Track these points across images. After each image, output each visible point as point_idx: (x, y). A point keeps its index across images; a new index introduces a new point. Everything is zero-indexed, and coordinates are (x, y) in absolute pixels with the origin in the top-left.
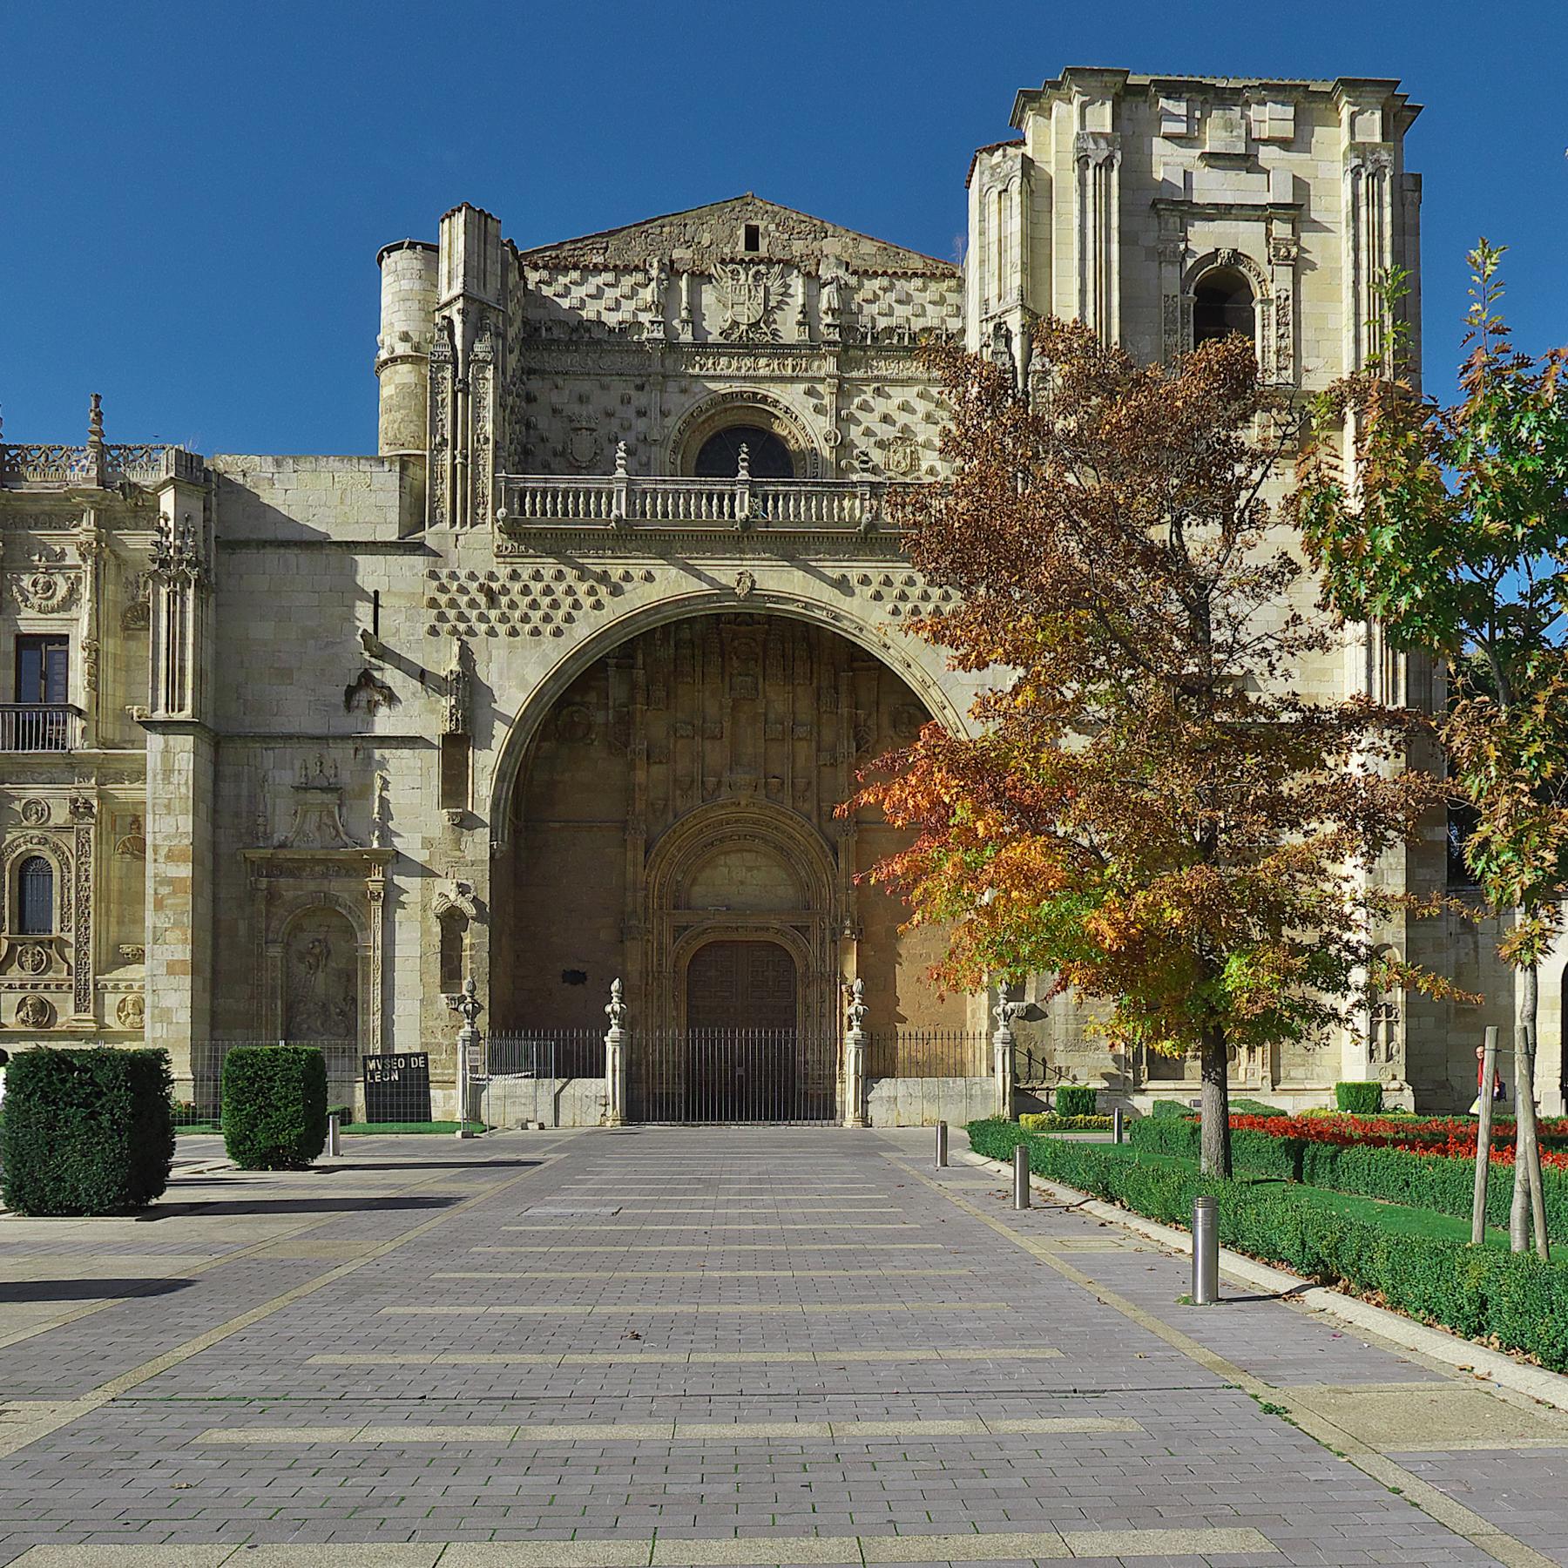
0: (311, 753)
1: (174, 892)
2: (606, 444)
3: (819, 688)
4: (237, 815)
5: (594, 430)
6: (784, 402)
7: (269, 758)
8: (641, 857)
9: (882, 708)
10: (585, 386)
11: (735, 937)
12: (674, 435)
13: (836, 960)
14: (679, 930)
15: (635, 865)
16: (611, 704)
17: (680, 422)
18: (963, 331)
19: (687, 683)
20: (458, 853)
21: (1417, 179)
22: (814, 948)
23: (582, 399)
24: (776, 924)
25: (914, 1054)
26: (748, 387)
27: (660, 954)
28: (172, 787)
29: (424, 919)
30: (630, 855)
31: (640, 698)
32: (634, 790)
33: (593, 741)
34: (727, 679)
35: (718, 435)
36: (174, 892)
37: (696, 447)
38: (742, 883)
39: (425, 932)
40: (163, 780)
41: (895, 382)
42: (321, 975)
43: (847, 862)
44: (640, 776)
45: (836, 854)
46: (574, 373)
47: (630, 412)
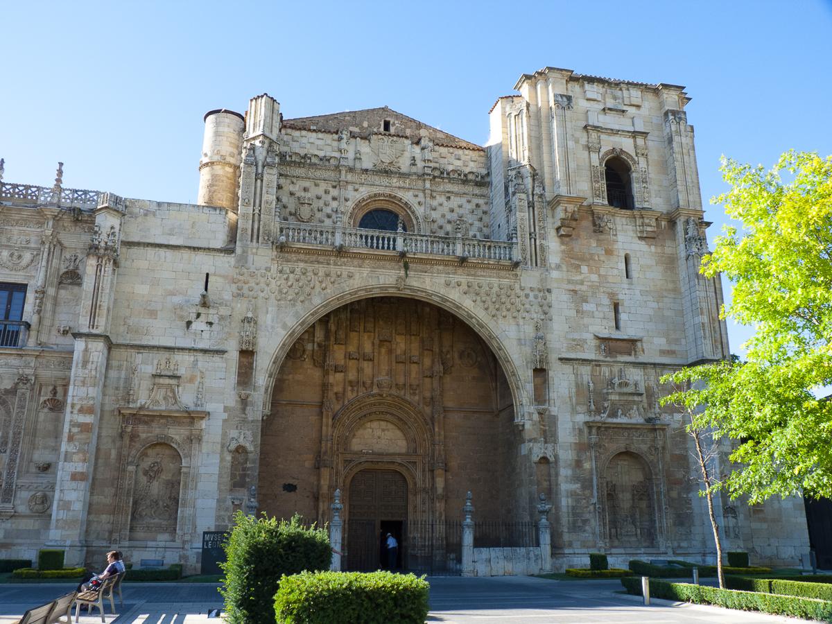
0: (163, 356)
1: (81, 431)
2: (316, 212)
4: (117, 388)
5: (311, 205)
6: (405, 199)
7: (139, 358)
9: (454, 349)
10: (307, 184)
11: (376, 467)
14: (347, 462)
15: (327, 426)
16: (316, 339)
17: (354, 205)
18: (488, 174)
19: (356, 331)
20: (244, 416)
21: (692, 127)
22: (419, 474)
24: (399, 461)
26: (388, 191)
28: (87, 371)
29: (222, 453)
30: (324, 420)
31: (332, 339)
32: (328, 386)
33: (305, 359)
34: (377, 330)
35: (370, 212)
36: (81, 431)
37: (360, 216)
38: (379, 438)
39: (222, 460)
40: (82, 367)
41: (457, 194)
42: (155, 484)
43: (439, 428)
44: (331, 379)
45: (433, 424)
46: (302, 178)
47: (329, 198)
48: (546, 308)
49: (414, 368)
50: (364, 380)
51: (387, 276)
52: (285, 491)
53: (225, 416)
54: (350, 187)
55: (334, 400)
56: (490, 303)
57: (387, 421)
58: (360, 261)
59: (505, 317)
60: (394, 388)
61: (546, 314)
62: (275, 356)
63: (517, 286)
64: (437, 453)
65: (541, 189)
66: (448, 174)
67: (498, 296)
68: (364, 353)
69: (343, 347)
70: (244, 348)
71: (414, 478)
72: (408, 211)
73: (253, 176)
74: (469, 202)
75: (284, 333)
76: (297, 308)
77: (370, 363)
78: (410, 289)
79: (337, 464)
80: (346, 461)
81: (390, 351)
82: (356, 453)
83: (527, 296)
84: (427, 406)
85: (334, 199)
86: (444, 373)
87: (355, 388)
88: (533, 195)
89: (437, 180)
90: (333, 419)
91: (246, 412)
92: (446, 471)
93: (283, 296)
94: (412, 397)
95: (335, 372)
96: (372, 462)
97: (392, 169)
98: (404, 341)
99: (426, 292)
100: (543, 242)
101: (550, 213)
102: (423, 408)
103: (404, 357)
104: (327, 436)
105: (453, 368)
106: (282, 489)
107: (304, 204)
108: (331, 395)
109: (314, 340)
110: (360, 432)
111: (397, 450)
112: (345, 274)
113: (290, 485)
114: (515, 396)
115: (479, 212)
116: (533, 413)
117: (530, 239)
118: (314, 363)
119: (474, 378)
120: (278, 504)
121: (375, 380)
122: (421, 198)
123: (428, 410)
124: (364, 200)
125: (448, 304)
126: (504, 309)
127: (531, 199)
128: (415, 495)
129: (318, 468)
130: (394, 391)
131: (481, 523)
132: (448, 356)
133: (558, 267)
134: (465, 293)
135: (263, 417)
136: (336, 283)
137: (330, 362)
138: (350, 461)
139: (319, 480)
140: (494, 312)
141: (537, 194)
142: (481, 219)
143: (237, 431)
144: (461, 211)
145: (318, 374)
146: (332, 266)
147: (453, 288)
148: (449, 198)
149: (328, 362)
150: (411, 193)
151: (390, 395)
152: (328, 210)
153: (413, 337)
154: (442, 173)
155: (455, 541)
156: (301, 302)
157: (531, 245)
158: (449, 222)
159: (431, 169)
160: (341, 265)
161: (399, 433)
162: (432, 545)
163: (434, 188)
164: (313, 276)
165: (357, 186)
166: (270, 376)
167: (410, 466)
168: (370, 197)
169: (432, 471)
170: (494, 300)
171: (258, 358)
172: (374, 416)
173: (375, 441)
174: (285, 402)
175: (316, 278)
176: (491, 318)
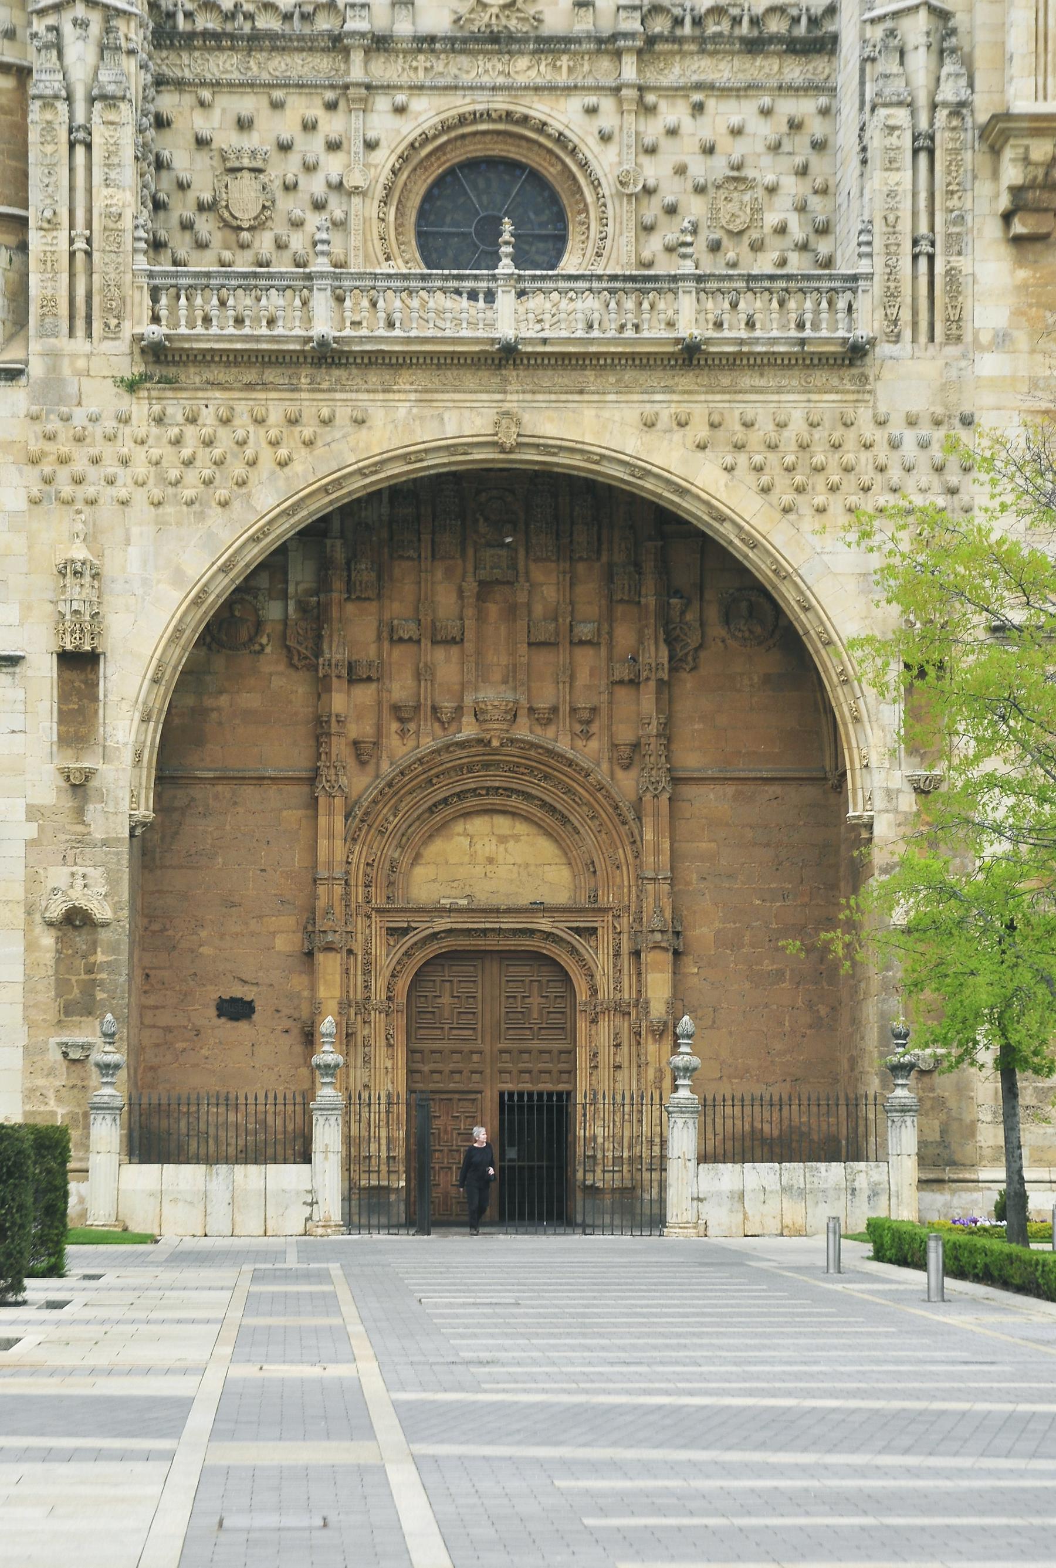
2: (279, 194)
3: (610, 565)
5: (259, 171)
6: (556, 125)
10: (248, 104)
11: (481, 943)
12: (385, 174)
13: (639, 981)
15: (331, 836)
16: (291, 589)
17: (394, 157)
19: (409, 558)
23: (244, 125)
24: (544, 924)
25: (758, 1125)
26: (500, 103)
27: (366, 972)
30: (322, 821)
31: (338, 584)
32: (328, 722)
34: (470, 552)
35: (451, 172)
38: (491, 861)
41: (725, 92)
43: (656, 832)
44: (339, 702)
48: (953, 478)
49: (586, 660)
51: (467, 413)
52: (223, 1020)
53: (31, 830)
54: (382, 103)
55: (351, 763)
56: (778, 471)
57: (514, 814)
58: (387, 375)
59: (821, 510)
60: (523, 720)
61: (953, 491)
62: (154, 662)
63: (864, 416)
64: (649, 905)
65: (963, 82)
66: (697, 22)
67: (803, 447)
68: (433, 622)
69: (373, 607)
70: (69, 647)
72: (568, 161)
73: (63, 136)
74: (766, 112)
75: (177, 595)
76: (209, 522)
77: (455, 650)
78: (537, 446)
79: (367, 941)
80: (391, 931)
81: (511, 612)
83: (895, 445)
84: (626, 768)
85: (333, 146)
86: (670, 670)
87: (412, 726)
88: (934, 107)
89: (659, 47)
90: (347, 818)
91: (87, 819)
92: (677, 953)
93: (170, 490)
94: (579, 743)
95: (351, 681)
96: (469, 931)
97: (513, 24)
99: (582, 452)
100: (956, 261)
101: (984, 160)
103: (552, 627)
105: (702, 654)
106: (213, 1012)
107: (240, 170)
108: (339, 748)
109: (285, 591)
110: (437, 847)
112: (343, 414)
113: (234, 1001)
114: (849, 742)
115: (801, 144)
116: (899, 791)
117: (915, 257)
118: (290, 658)
119: (767, 679)
120: (204, 1052)
121: (468, 700)
122: (608, 119)
123: (627, 783)
124: (426, 139)
125: (649, 484)
126: (821, 487)
127: (923, 125)
128: (594, 1021)
129: (310, 954)
130: (523, 731)
131: (785, 1098)
133: (1002, 340)
134: (702, 447)
135: (132, 829)
136: (319, 443)
137: (336, 653)
140: (788, 498)
141: (945, 104)
142: (803, 171)
143: (66, 870)
144: (738, 149)
145: (300, 691)
146: (304, 395)
147: (665, 432)
148: (699, 108)
149: (328, 656)
150: (574, 105)
151: (512, 741)
152: (316, 186)
153: (581, 568)
154: (678, 22)
156: (220, 503)
157: (915, 278)
158: (700, 190)
159: (637, 15)
160: (329, 390)
161: (546, 847)
163: (652, 77)
164: (251, 429)
165: (401, 98)
166: (145, 719)
167: (575, 940)
168: (446, 127)
169: (637, 954)
170: (790, 459)
171: (109, 673)
172: (471, 802)
173: (479, 870)
174: (211, 775)
175: (262, 431)
176: (778, 515)
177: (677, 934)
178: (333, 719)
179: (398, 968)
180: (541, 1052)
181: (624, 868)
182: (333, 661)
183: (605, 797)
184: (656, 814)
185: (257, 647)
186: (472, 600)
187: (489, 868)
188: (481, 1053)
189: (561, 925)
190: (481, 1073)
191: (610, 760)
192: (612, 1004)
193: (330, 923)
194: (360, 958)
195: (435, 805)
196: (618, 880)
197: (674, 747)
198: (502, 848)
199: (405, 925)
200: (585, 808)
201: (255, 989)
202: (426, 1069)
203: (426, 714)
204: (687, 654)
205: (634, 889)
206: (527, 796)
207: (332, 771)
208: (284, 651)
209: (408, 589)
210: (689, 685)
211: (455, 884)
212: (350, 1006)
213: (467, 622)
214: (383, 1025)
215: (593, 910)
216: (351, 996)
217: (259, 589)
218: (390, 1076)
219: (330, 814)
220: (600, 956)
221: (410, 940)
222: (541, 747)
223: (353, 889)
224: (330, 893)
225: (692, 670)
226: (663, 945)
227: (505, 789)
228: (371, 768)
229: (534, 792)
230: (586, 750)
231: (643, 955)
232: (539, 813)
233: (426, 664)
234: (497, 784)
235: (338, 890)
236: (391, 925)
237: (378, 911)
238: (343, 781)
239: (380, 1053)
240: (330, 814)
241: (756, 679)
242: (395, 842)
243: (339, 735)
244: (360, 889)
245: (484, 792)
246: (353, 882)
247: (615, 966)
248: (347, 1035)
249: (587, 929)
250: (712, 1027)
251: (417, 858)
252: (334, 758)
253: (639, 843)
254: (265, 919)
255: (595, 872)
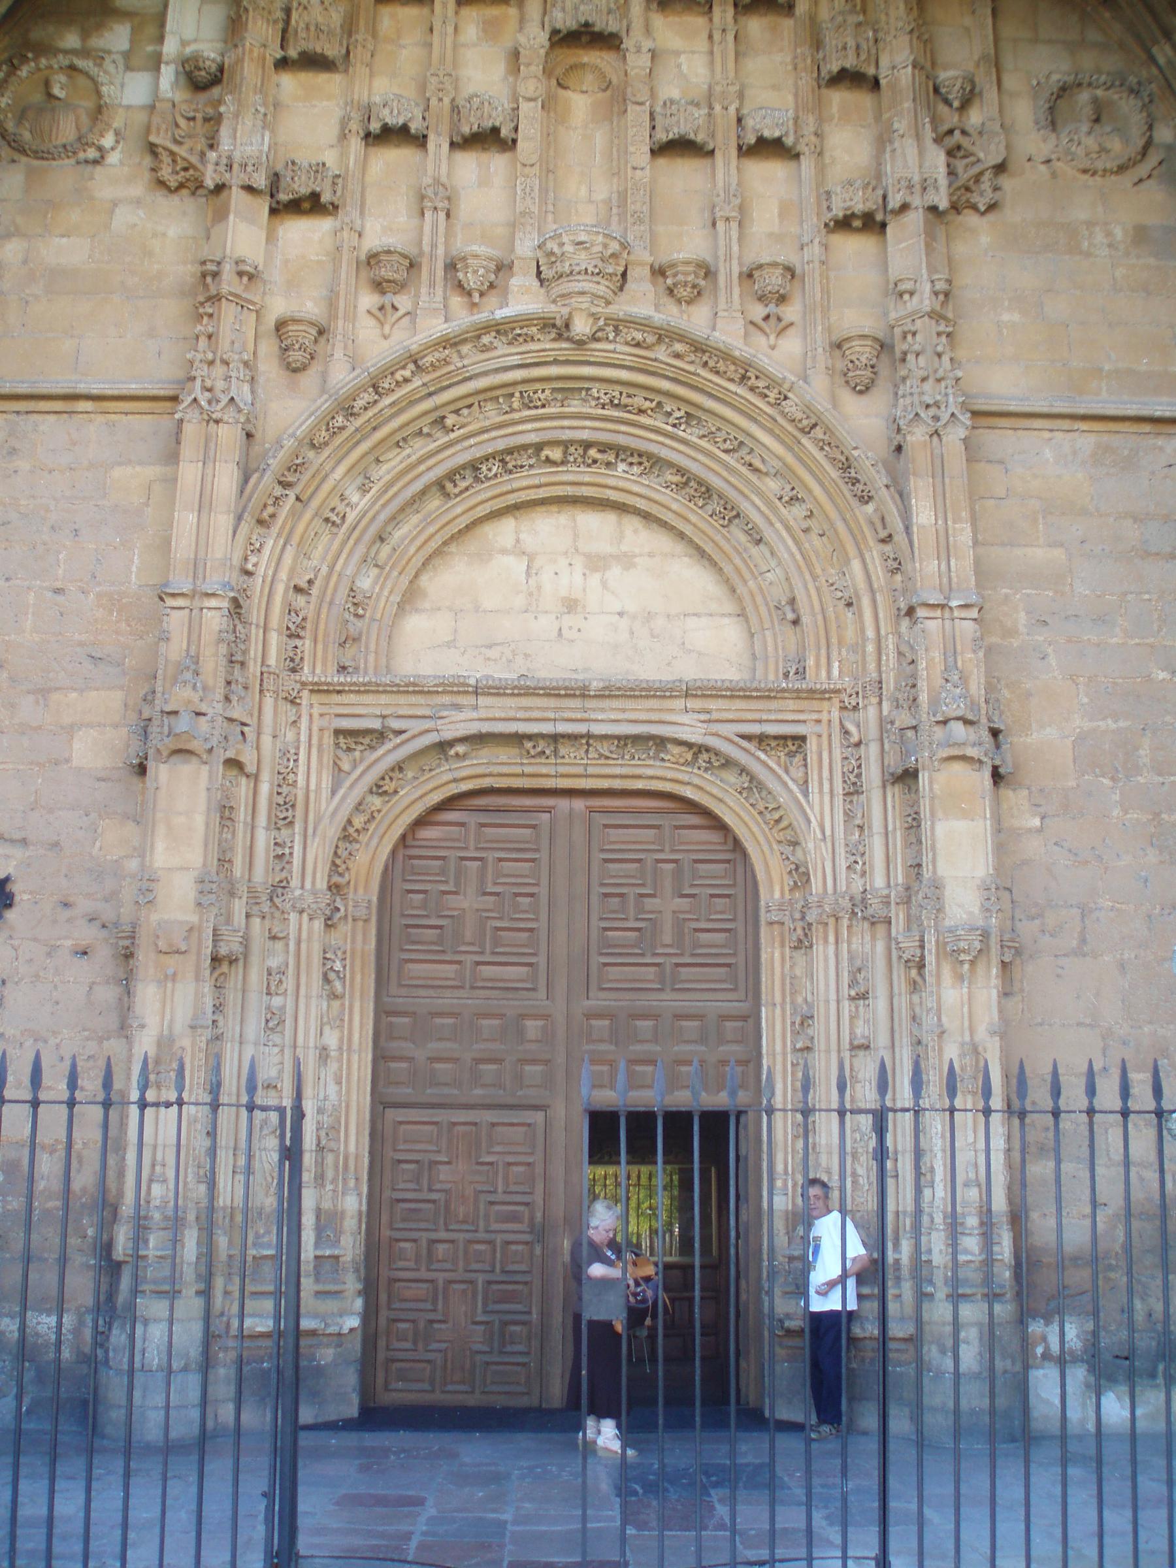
8: (226, 479)
9: (1010, 82)
15: (204, 504)
16: (170, 47)
30: (189, 472)
38: (571, 605)
50: (461, 245)
55: (269, 368)
64: (930, 665)
68: (455, 109)
71: (795, 844)
77: (497, 162)
79: (288, 755)
82: (414, 688)
87: (403, 302)
92: (997, 776)
94: (761, 340)
96: (517, 739)
98: (702, 44)
102: (835, 402)
104: (197, 566)
111: (688, 671)
119: (1141, 235)
128: (803, 944)
129: (142, 770)
132: (975, 117)
138: (381, 735)
139: (142, 851)
145: (173, 232)
149: (225, 145)
151: (618, 324)
155: (1076, 1236)
162: (920, 1267)
167: (763, 763)
169: (907, 777)
173: (545, 625)
177: (995, 733)
178: (228, 269)
179: (358, 821)
180: (679, 1017)
181: (866, 602)
182: (237, 156)
183: (822, 445)
184: (939, 469)
185: (92, 154)
186: (537, 69)
187: (568, 621)
188: (546, 1017)
189: (729, 730)
190: (547, 1062)
191: (830, 370)
192: (846, 903)
193: (187, 693)
194: (265, 788)
195: (451, 476)
196: (850, 634)
197: (961, 354)
198: (595, 579)
199: (376, 724)
200: (772, 486)
201: (18, 853)
202: (420, 1055)
203: (432, 273)
204: (977, 178)
205: (890, 643)
206: (651, 462)
207: (219, 370)
208: (148, 161)
209: (408, 55)
210: (985, 240)
211: (494, 653)
212: (232, 894)
213: (525, 107)
214: (317, 948)
215: (798, 694)
216: (238, 870)
217: (109, 52)
218: (333, 1066)
219: (207, 458)
220: (814, 797)
221: (387, 755)
222: (682, 338)
223: (256, 634)
224: (193, 629)
225: (992, 207)
226: (971, 752)
227: (604, 448)
228: (309, 380)
229: (664, 453)
230: (775, 353)
231: (924, 777)
232: (673, 503)
233: (437, 182)
234: (585, 435)
235: (214, 619)
236: (346, 724)
237: (318, 689)
238: (243, 393)
239: (313, 1006)
240: (207, 458)
241: (1118, 233)
242: (361, 550)
243: (242, 304)
244: (274, 637)
245: (556, 454)
246: (255, 615)
247: (848, 816)
248: (216, 960)
249: (783, 738)
250: (1078, 952)
251: (410, 598)
252: (224, 344)
253: (900, 538)
254: (55, 697)
255: (796, 622)
